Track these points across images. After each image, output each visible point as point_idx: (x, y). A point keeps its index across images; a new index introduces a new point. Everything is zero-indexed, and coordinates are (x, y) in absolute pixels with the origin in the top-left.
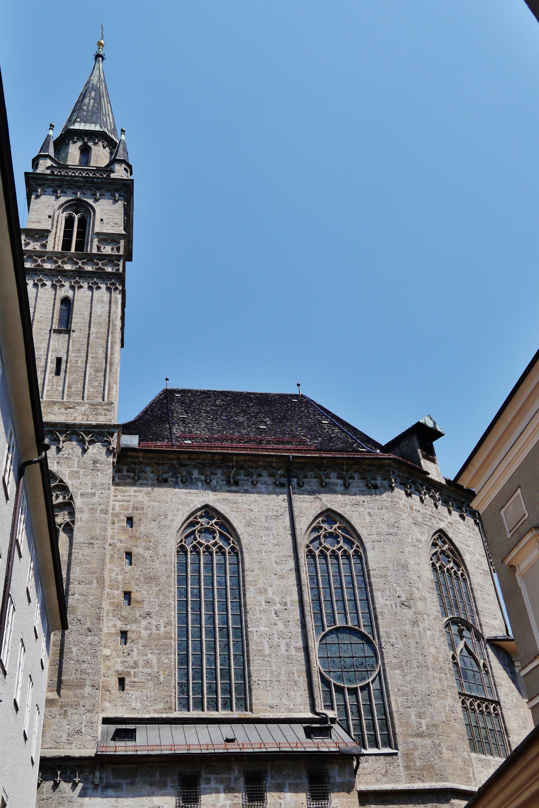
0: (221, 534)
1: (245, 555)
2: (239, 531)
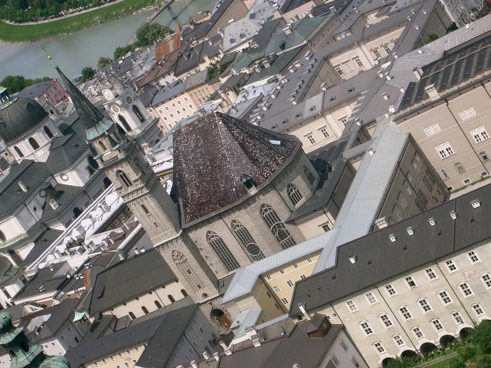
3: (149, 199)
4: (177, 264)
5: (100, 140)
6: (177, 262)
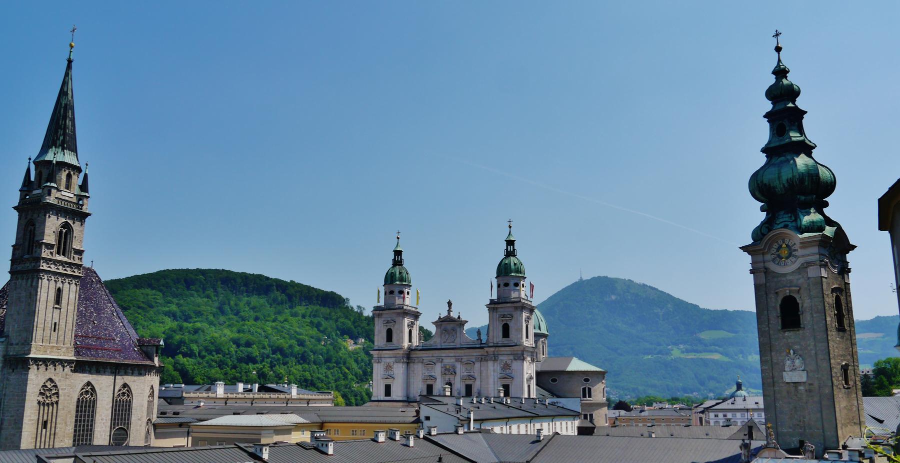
0: (91, 393)
1: (98, 402)
2: (97, 392)
3: (73, 286)
4: (39, 403)
5: (72, 173)
6: (40, 399)
